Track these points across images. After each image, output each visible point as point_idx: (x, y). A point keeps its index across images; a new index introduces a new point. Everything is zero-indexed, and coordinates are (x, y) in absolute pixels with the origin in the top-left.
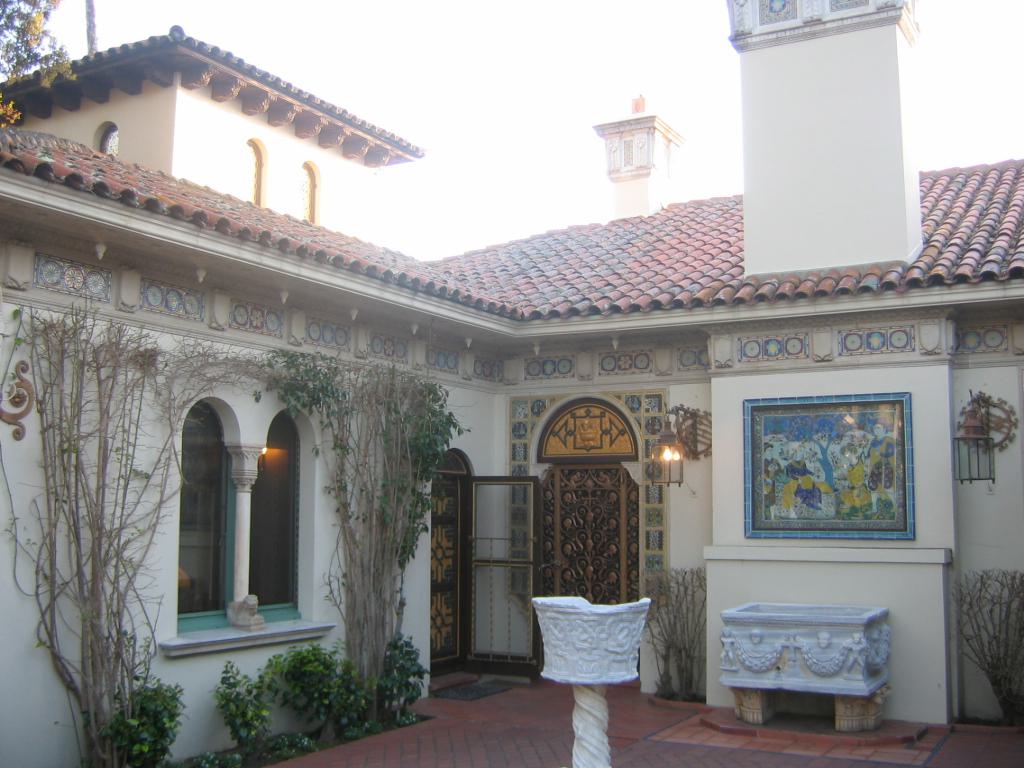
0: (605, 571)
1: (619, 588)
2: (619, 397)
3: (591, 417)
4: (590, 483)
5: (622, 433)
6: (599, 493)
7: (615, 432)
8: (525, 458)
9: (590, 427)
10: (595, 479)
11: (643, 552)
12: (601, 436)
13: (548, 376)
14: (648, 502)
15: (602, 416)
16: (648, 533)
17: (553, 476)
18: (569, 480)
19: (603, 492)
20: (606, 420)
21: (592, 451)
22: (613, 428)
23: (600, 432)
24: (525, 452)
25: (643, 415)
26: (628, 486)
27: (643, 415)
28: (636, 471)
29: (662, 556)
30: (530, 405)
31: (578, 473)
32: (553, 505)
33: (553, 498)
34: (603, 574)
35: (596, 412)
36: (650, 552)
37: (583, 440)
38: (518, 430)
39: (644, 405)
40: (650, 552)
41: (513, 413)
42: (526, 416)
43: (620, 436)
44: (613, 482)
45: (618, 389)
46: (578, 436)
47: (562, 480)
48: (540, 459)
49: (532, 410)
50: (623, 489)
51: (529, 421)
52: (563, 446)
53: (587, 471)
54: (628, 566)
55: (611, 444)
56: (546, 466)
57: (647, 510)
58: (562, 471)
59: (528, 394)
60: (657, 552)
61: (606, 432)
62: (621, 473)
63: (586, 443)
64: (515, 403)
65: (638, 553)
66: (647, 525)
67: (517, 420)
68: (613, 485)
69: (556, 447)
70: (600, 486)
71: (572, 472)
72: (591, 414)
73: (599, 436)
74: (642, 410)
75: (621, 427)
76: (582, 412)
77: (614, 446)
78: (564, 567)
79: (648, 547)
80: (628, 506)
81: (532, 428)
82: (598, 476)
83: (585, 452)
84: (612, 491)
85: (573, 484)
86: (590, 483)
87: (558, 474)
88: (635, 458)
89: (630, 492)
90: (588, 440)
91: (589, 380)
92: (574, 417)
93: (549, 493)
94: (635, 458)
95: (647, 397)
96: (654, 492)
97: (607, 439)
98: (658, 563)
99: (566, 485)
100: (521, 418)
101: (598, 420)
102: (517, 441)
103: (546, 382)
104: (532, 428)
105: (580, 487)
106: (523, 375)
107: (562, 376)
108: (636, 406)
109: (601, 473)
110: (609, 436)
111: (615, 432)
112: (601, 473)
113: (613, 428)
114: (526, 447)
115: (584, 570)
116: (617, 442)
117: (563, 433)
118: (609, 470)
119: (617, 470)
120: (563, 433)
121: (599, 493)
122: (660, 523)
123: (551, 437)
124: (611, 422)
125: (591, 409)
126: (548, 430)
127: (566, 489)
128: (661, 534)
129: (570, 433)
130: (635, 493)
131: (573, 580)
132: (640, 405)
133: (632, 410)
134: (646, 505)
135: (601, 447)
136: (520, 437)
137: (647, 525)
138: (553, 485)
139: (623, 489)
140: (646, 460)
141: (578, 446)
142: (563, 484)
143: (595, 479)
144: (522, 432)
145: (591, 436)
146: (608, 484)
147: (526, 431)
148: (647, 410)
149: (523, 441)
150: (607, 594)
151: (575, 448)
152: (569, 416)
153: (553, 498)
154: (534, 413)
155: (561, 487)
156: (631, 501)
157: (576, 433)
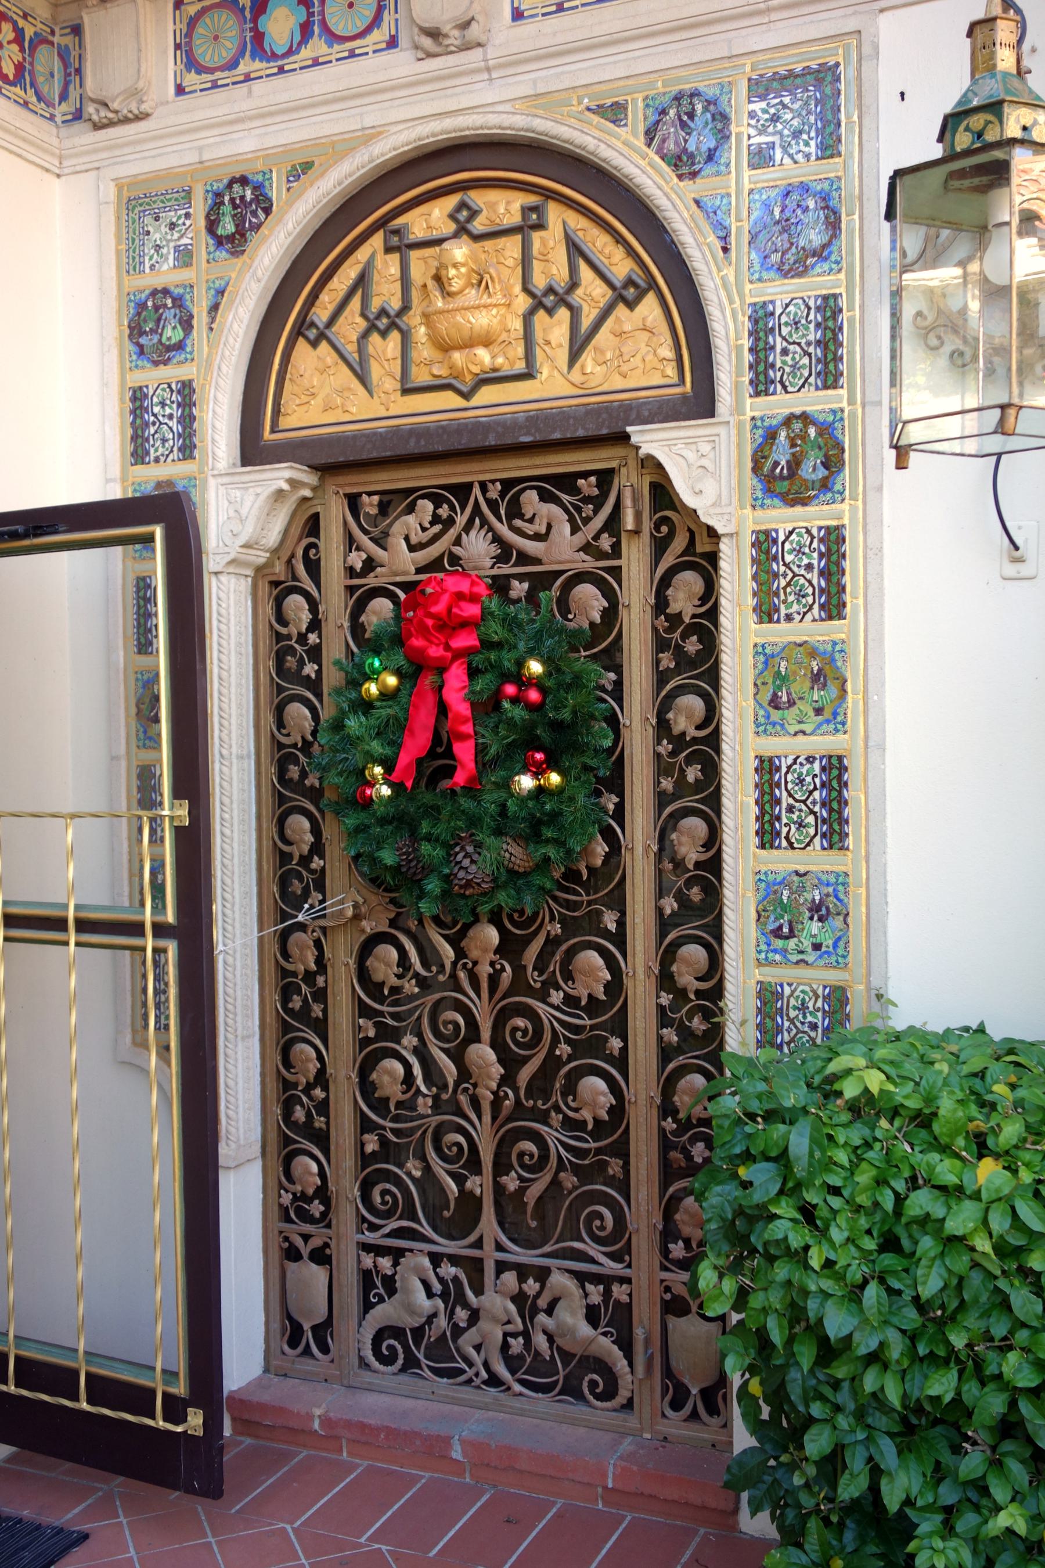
0: (552, 942)
1: (620, 1027)
2: (614, 112)
3: (477, 238)
4: (478, 548)
5: (625, 295)
6: (519, 589)
7: (592, 292)
8: (188, 450)
9: (480, 281)
10: (503, 530)
11: (743, 862)
12: (528, 318)
13: (279, 61)
14: (766, 613)
15: (531, 223)
16: (767, 767)
17: (313, 526)
18: (380, 541)
19: (541, 581)
20: (550, 243)
21: (487, 395)
22: (585, 273)
23: (523, 302)
24: (188, 420)
25: (742, 187)
26: (660, 547)
27: (742, 187)
28: (705, 468)
29: (841, 881)
30: (200, 208)
31: (426, 507)
32: (315, 653)
33: (315, 625)
34: (541, 965)
35: (503, 207)
36: (781, 862)
37: (445, 347)
38: (153, 325)
39: (744, 132)
40: (781, 862)
41: (132, 259)
42: (185, 257)
43: (621, 310)
44: (579, 539)
45: (605, 71)
46: (421, 332)
47: (351, 543)
48: (253, 451)
49: (212, 226)
50: (636, 562)
51: (197, 279)
52: (355, 384)
53: (462, 491)
54: (664, 924)
55: (574, 356)
56: (279, 475)
57: (760, 650)
58: (353, 502)
59: (191, 158)
60: (817, 860)
61: (545, 301)
62: (630, 484)
63: (457, 356)
64: (140, 206)
65: (713, 865)
66: (764, 727)
67: (151, 281)
68: (586, 548)
69: (322, 396)
70: (524, 558)
71: (393, 502)
72: (478, 225)
73: (517, 325)
74: (735, 154)
75: (621, 267)
76: (432, 218)
77: (588, 359)
78: (368, 927)
79: (768, 835)
80: (661, 645)
81: (215, 308)
82: (515, 511)
83: (450, 400)
84: (580, 577)
85: (401, 561)
86: (478, 548)
87: (335, 514)
88: (700, 403)
89: (665, 582)
90: (468, 344)
91: (466, 47)
92: (401, 246)
93: (296, 600)
94: (700, 403)
95: (759, 88)
96: (801, 564)
97: (555, 330)
98: (819, 911)
99: (370, 565)
100: (166, 273)
101: (512, 246)
102: (152, 377)
103: (270, 90)
104: (215, 308)
105: (435, 565)
106: (162, 68)
107: (340, 49)
108: (700, 141)
109: (530, 499)
110: (563, 314)
111: (592, 292)
112: (530, 499)
113: (585, 273)
114: (186, 392)
115: (458, 1056)
116: (604, 335)
117: (350, 327)
118: (567, 482)
119: (605, 478)
120: (350, 327)
121: (519, 589)
122: (832, 716)
123: (301, 344)
124: (575, 249)
125: (478, 198)
126: (287, 320)
127: (371, 581)
128: (835, 769)
129: (386, 322)
130: (690, 582)
131: (411, 987)
132: (723, 136)
133: (684, 165)
134: (757, 632)
135: (528, 375)
136: (166, 353)
137: (764, 727)
138: (313, 568)
139: (636, 562)
140: (754, 407)
141: (420, 376)
142: (357, 560)
143: (503, 530)
144: (172, 333)
145: (491, 326)
146: (563, 548)
147: (187, 324)
148: (761, 158)
149: (173, 373)
150: (564, 1050)
151: (406, 391)
152: (377, 241)
153: (315, 625)
154: (220, 241)
155: (351, 572)
156: (675, 619)
157: (414, 319)
